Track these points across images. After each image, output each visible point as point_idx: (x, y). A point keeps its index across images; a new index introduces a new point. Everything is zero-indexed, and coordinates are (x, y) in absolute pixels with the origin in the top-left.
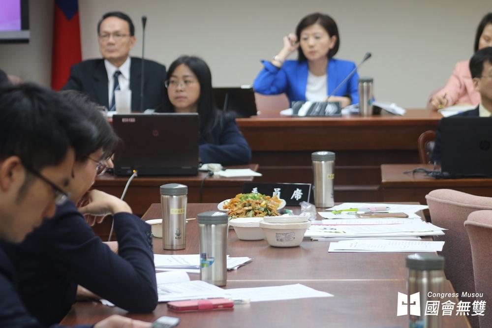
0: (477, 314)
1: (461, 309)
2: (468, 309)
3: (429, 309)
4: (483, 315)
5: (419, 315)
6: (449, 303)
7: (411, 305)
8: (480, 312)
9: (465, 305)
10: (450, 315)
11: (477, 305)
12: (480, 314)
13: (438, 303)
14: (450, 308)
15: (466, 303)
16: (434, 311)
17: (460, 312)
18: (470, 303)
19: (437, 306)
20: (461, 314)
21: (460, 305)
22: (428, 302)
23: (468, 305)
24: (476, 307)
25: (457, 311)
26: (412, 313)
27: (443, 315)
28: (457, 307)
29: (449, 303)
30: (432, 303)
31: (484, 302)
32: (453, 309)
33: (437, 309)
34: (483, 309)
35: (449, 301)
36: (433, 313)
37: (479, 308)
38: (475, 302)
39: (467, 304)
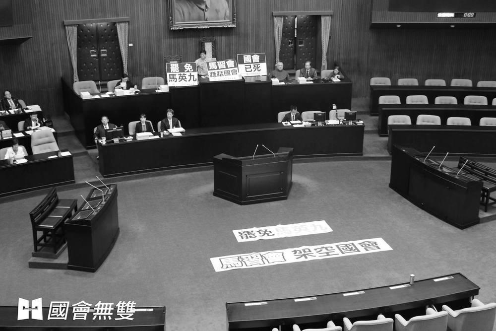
0: (124, 318)
1: (100, 312)
2: (109, 311)
3: (53, 312)
4: (132, 319)
5: (42, 319)
10: (85, 319)
14: (84, 311)
15: (107, 304)
16: (61, 314)
17: (98, 316)
18: (113, 304)
19: (66, 308)
20: (100, 318)
21: (99, 307)
22: (52, 303)
23: (110, 306)
24: (122, 309)
27: (74, 319)
30: (59, 304)
31: (133, 303)
33: (65, 312)
36: (60, 316)
37: (126, 311)
38: (120, 303)
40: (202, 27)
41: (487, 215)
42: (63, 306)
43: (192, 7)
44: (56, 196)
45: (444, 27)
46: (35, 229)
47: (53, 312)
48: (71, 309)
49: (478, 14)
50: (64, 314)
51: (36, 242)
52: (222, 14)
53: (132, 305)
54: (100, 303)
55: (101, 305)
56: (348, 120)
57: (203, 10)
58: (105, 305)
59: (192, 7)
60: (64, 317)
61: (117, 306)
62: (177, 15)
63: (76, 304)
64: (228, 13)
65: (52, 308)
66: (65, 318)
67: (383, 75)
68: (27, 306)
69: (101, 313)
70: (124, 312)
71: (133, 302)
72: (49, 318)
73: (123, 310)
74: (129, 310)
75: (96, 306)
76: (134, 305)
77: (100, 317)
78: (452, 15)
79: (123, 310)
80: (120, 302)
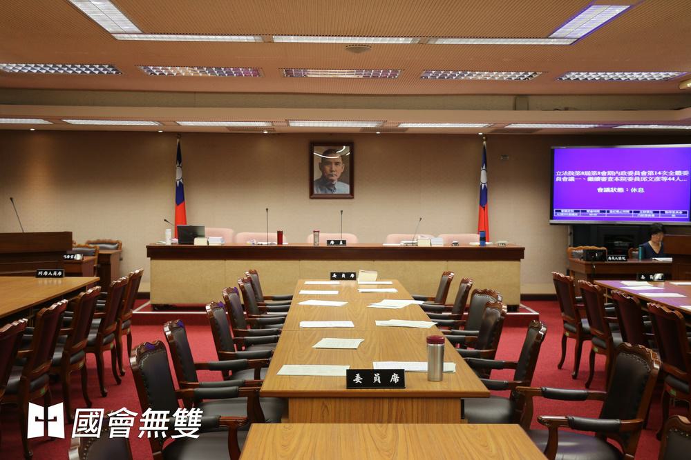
0: (184, 435)
1: (149, 425)
2: (163, 424)
4: (196, 437)
5: (62, 436)
6: (124, 412)
7: (43, 418)
8: (190, 431)
9: (159, 416)
10: (127, 436)
11: (183, 416)
12: (189, 435)
13: (100, 413)
14: (126, 424)
15: (159, 413)
16: (91, 428)
18: (168, 412)
19: (98, 419)
20: (149, 436)
21: (147, 417)
23: (165, 416)
24: (182, 421)
25: (141, 428)
26: (51, 434)
27: (112, 436)
28: (142, 420)
29: (124, 412)
30: (88, 413)
31: (199, 411)
32: (131, 424)
33: (97, 425)
34: (195, 425)
35: (124, 409)
36: (90, 432)
37: (187, 423)
38: (179, 411)
39: (162, 415)
42: (94, 416)
47: (80, 425)
48: (106, 420)
50: (96, 428)
53: (197, 414)
54: (149, 411)
55: (150, 415)
58: (156, 415)
60: (96, 433)
61: (174, 416)
63: (114, 414)
65: (79, 418)
66: (98, 436)
68: (42, 417)
69: (151, 428)
70: (185, 425)
71: (198, 409)
72: (74, 435)
73: (184, 423)
74: (193, 423)
75: (143, 415)
76: (199, 414)
77: (149, 433)
79: (184, 423)
80: (179, 409)
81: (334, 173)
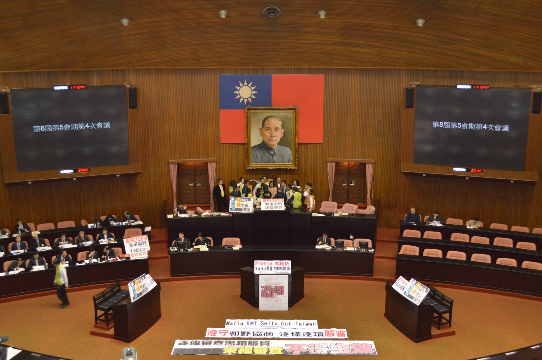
40: (270, 168)
41: (439, 332)
43: (264, 153)
44: (119, 286)
45: (459, 178)
46: (97, 308)
49: (484, 170)
51: (97, 318)
52: (286, 159)
56: (361, 248)
57: (272, 155)
59: (264, 153)
62: (252, 157)
64: (291, 158)
67: (68, 220)
78: (464, 170)
81: (274, 138)
